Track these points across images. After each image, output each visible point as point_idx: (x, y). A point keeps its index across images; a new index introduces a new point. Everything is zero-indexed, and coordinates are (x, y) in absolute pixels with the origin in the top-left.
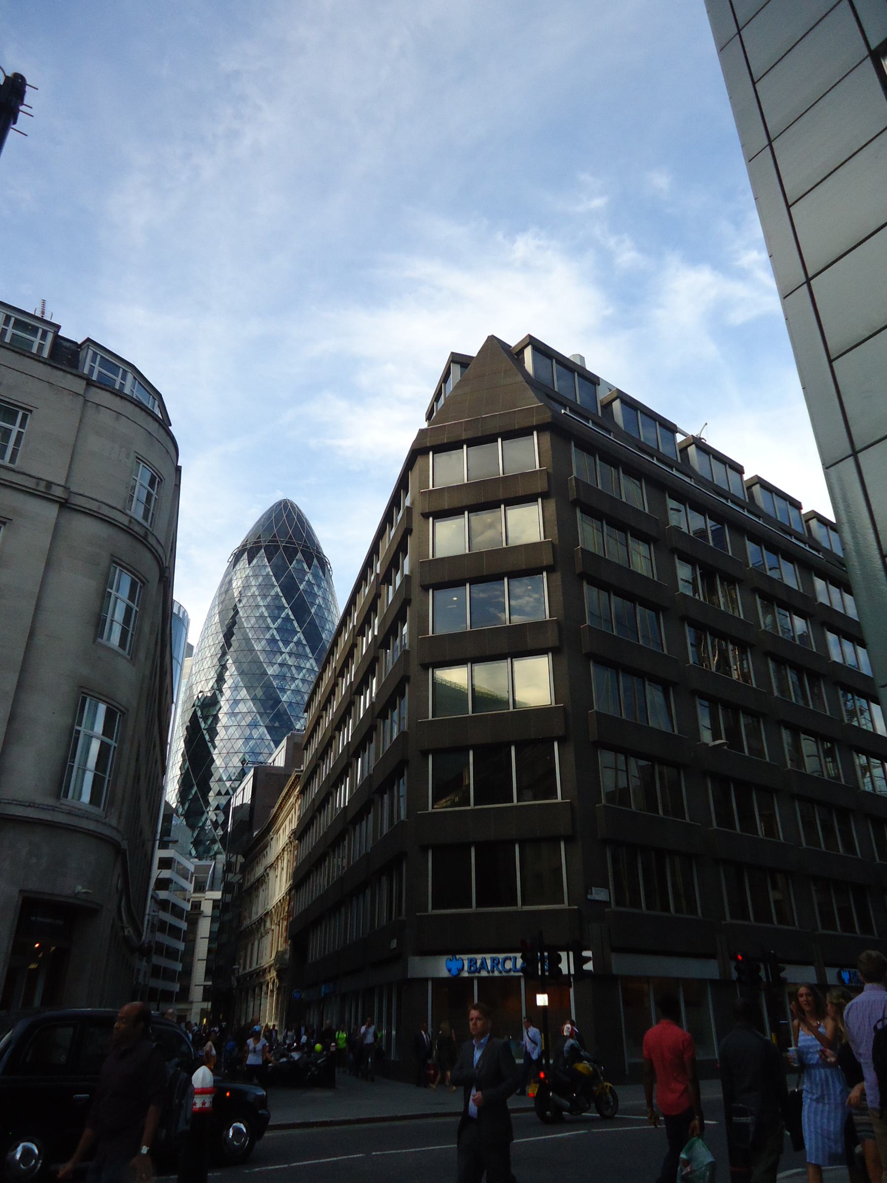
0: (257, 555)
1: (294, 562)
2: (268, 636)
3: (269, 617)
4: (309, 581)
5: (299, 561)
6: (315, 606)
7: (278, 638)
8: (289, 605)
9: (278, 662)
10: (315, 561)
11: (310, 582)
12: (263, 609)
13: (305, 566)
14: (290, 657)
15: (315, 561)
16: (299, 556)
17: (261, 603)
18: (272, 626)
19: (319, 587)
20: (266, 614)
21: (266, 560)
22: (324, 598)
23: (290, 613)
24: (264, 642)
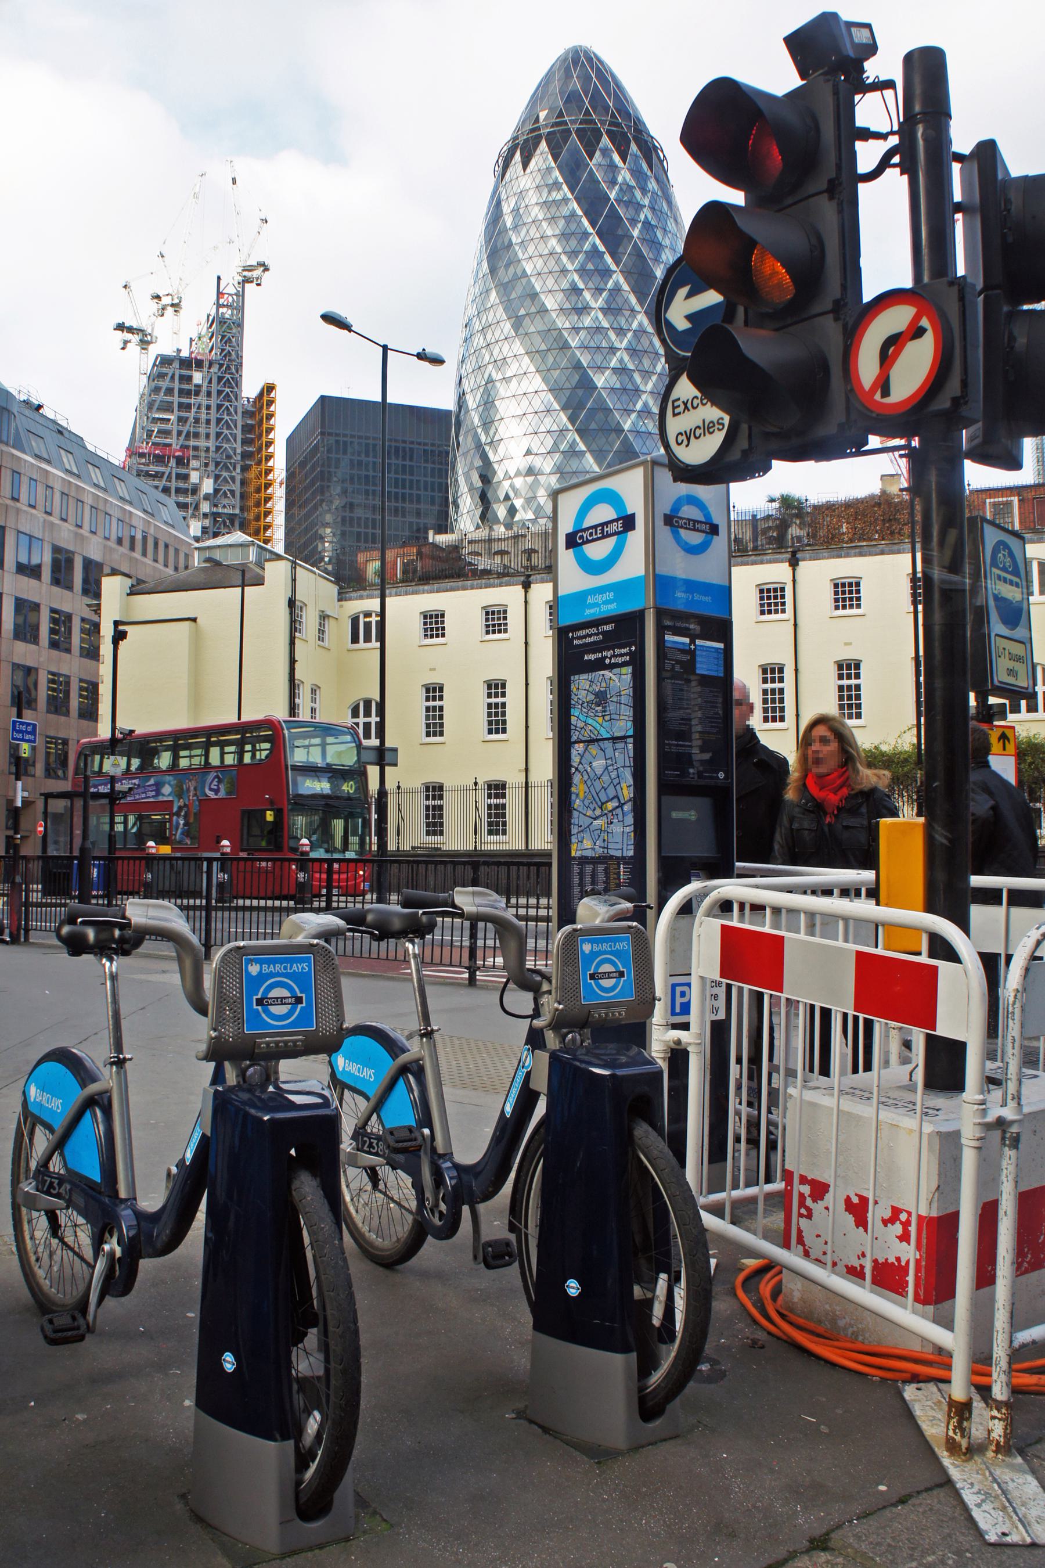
0: (535, 151)
1: (598, 154)
2: (565, 285)
3: (565, 253)
4: (625, 182)
5: (605, 152)
6: (640, 225)
7: (581, 286)
8: (594, 228)
9: (612, 365)
10: (634, 148)
11: (650, 223)
12: (553, 242)
13: (616, 158)
14: (605, 315)
15: (634, 148)
16: (605, 141)
17: (549, 232)
18: (570, 267)
19: (644, 191)
20: (559, 249)
21: (550, 157)
22: (653, 209)
23: (598, 241)
24: (560, 296)
